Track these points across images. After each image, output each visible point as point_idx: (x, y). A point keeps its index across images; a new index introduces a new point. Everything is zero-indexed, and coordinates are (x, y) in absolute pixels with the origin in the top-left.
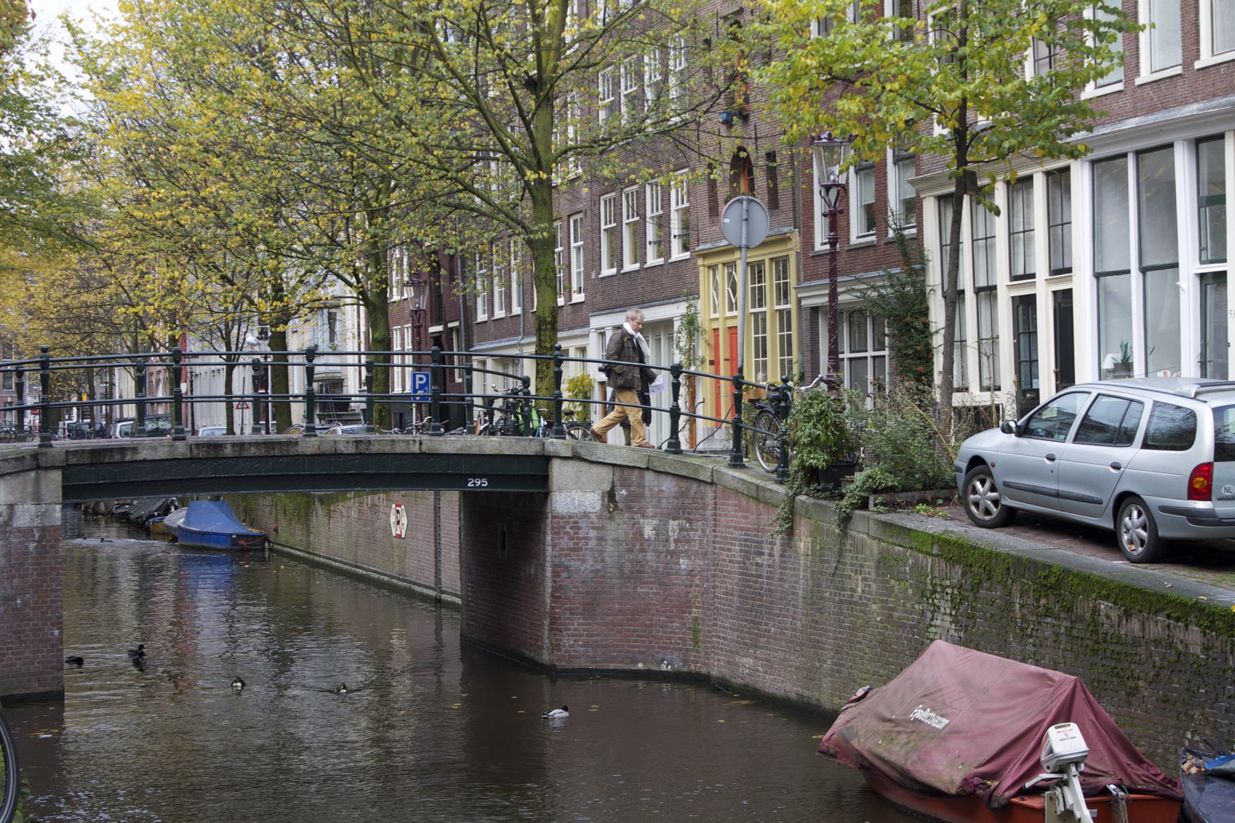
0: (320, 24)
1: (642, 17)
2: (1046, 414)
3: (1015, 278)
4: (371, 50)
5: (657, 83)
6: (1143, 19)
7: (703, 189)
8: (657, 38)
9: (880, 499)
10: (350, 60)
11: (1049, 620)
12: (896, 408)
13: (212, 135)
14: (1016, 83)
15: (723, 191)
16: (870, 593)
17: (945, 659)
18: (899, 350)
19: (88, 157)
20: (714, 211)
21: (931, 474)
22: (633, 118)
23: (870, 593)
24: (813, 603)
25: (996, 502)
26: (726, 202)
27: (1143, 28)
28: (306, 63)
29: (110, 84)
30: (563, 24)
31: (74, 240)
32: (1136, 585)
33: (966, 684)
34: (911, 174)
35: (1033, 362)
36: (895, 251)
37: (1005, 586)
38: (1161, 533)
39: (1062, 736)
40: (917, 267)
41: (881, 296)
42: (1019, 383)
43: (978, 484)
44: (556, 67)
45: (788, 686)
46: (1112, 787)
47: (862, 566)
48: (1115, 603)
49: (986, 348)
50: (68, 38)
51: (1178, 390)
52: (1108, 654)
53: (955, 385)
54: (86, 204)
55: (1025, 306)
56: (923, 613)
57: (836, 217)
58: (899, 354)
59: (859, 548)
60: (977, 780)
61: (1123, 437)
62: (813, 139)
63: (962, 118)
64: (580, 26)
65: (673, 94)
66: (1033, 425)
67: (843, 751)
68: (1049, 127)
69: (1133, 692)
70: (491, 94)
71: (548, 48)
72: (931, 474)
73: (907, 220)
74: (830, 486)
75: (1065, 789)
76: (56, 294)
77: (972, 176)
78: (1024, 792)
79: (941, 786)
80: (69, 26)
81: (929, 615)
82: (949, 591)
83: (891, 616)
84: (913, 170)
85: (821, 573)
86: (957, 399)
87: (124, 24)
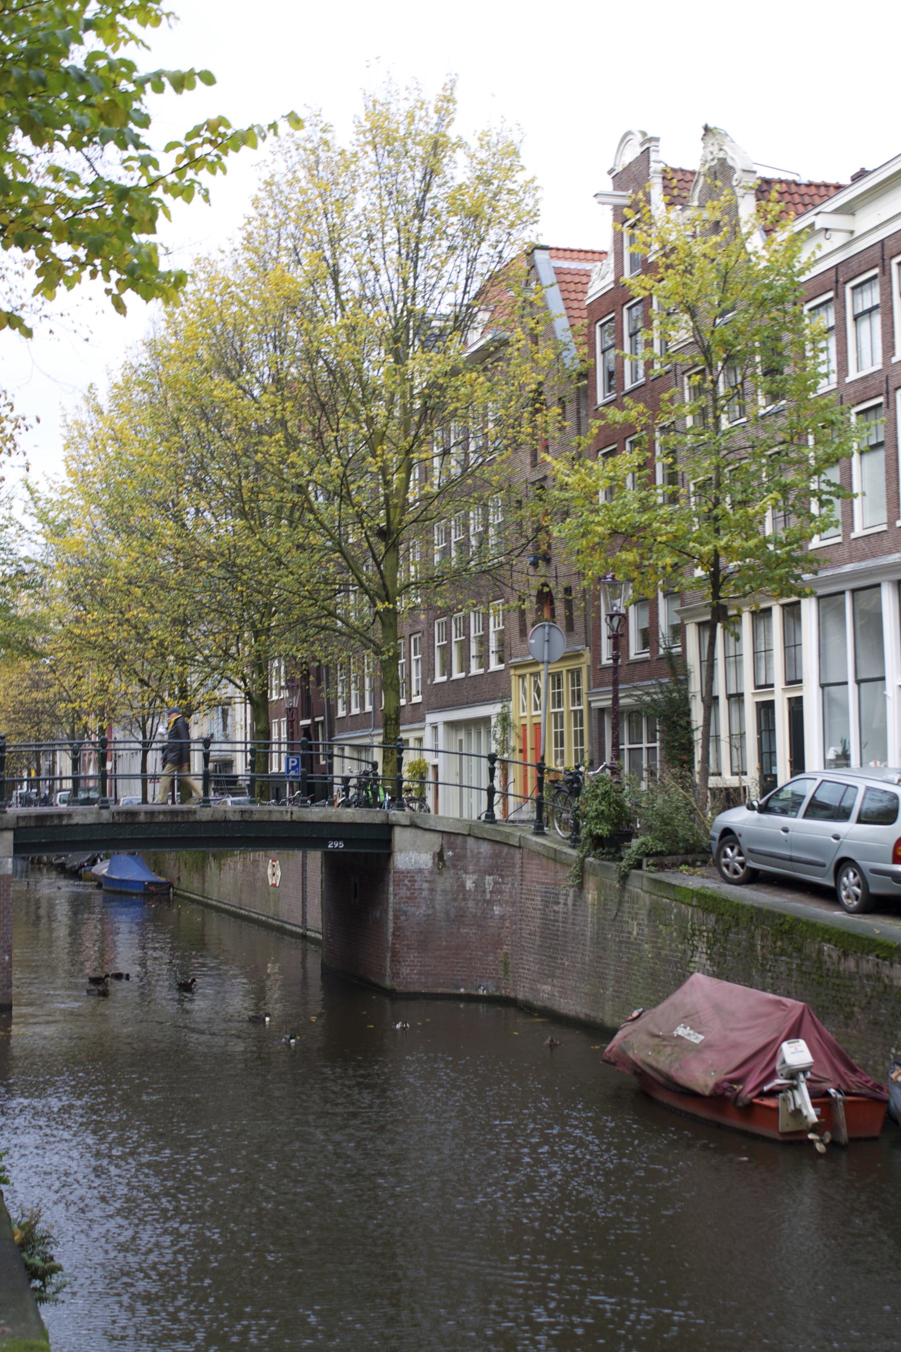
0: (220, 487)
1: (470, 481)
2: (782, 796)
3: (758, 687)
4: (258, 507)
5: (479, 533)
6: (856, 489)
7: (515, 616)
8: (480, 498)
9: (651, 861)
10: (243, 514)
11: (784, 958)
12: (664, 788)
13: (134, 572)
14: (761, 537)
15: (530, 618)
16: (643, 935)
17: (702, 988)
18: (668, 743)
19: (40, 586)
20: (523, 633)
21: (691, 842)
22: (460, 561)
23: (643, 935)
24: (598, 943)
25: (742, 865)
26: (533, 626)
27: (856, 496)
28: (208, 515)
29: (58, 531)
30: (407, 488)
31: (28, 651)
32: (852, 931)
33: (717, 1008)
34: (677, 606)
35: (772, 753)
36: (665, 665)
37: (749, 931)
38: (872, 890)
39: (793, 1050)
40: (682, 678)
41: (653, 700)
42: (761, 769)
43: (728, 850)
44: (401, 521)
45: (579, 1008)
46: (832, 1091)
47: (637, 914)
48: (836, 946)
49: (736, 742)
50: (27, 495)
51: (884, 778)
52: (830, 985)
53: (711, 771)
54: (39, 625)
55: (766, 709)
56: (684, 952)
57: (619, 640)
58: (667, 746)
59: (635, 899)
60: (726, 1085)
61: (841, 814)
62: (600, 579)
63: (716, 564)
64: (421, 489)
65: (492, 542)
66: (772, 804)
67: (621, 1059)
68: (783, 577)
69: (850, 1016)
70: (351, 541)
71: (396, 506)
72: (691, 842)
73: (674, 642)
74: (613, 850)
75: (796, 1092)
76: (13, 692)
77: (724, 608)
78: (762, 1095)
79: (698, 1089)
80: (28, 487)
81: (690, 953)
82: (705, 934)
83: (660, 954)
84: (679, 602)
85: (605, 919)
86: (713, 782)
87: (69, 485)
